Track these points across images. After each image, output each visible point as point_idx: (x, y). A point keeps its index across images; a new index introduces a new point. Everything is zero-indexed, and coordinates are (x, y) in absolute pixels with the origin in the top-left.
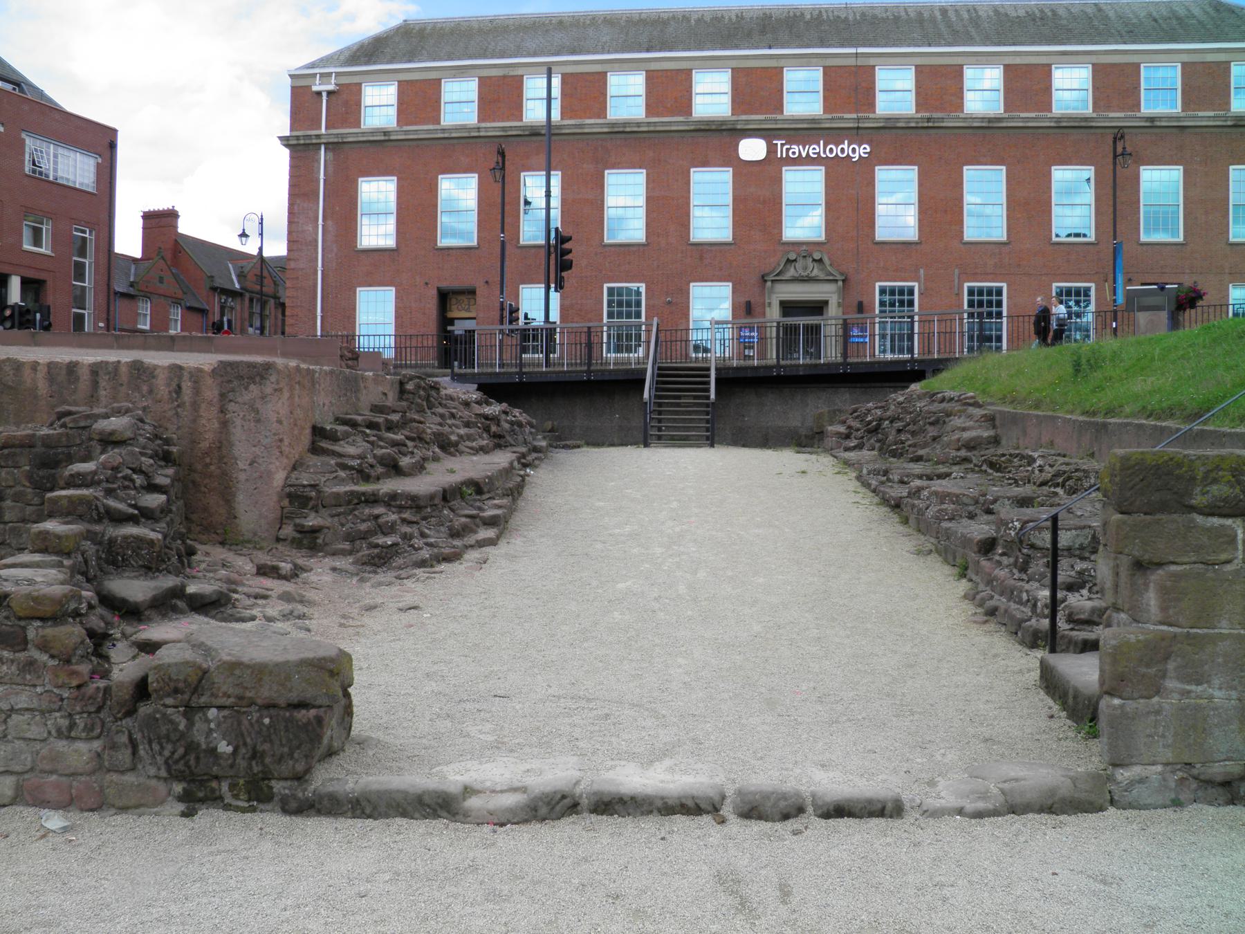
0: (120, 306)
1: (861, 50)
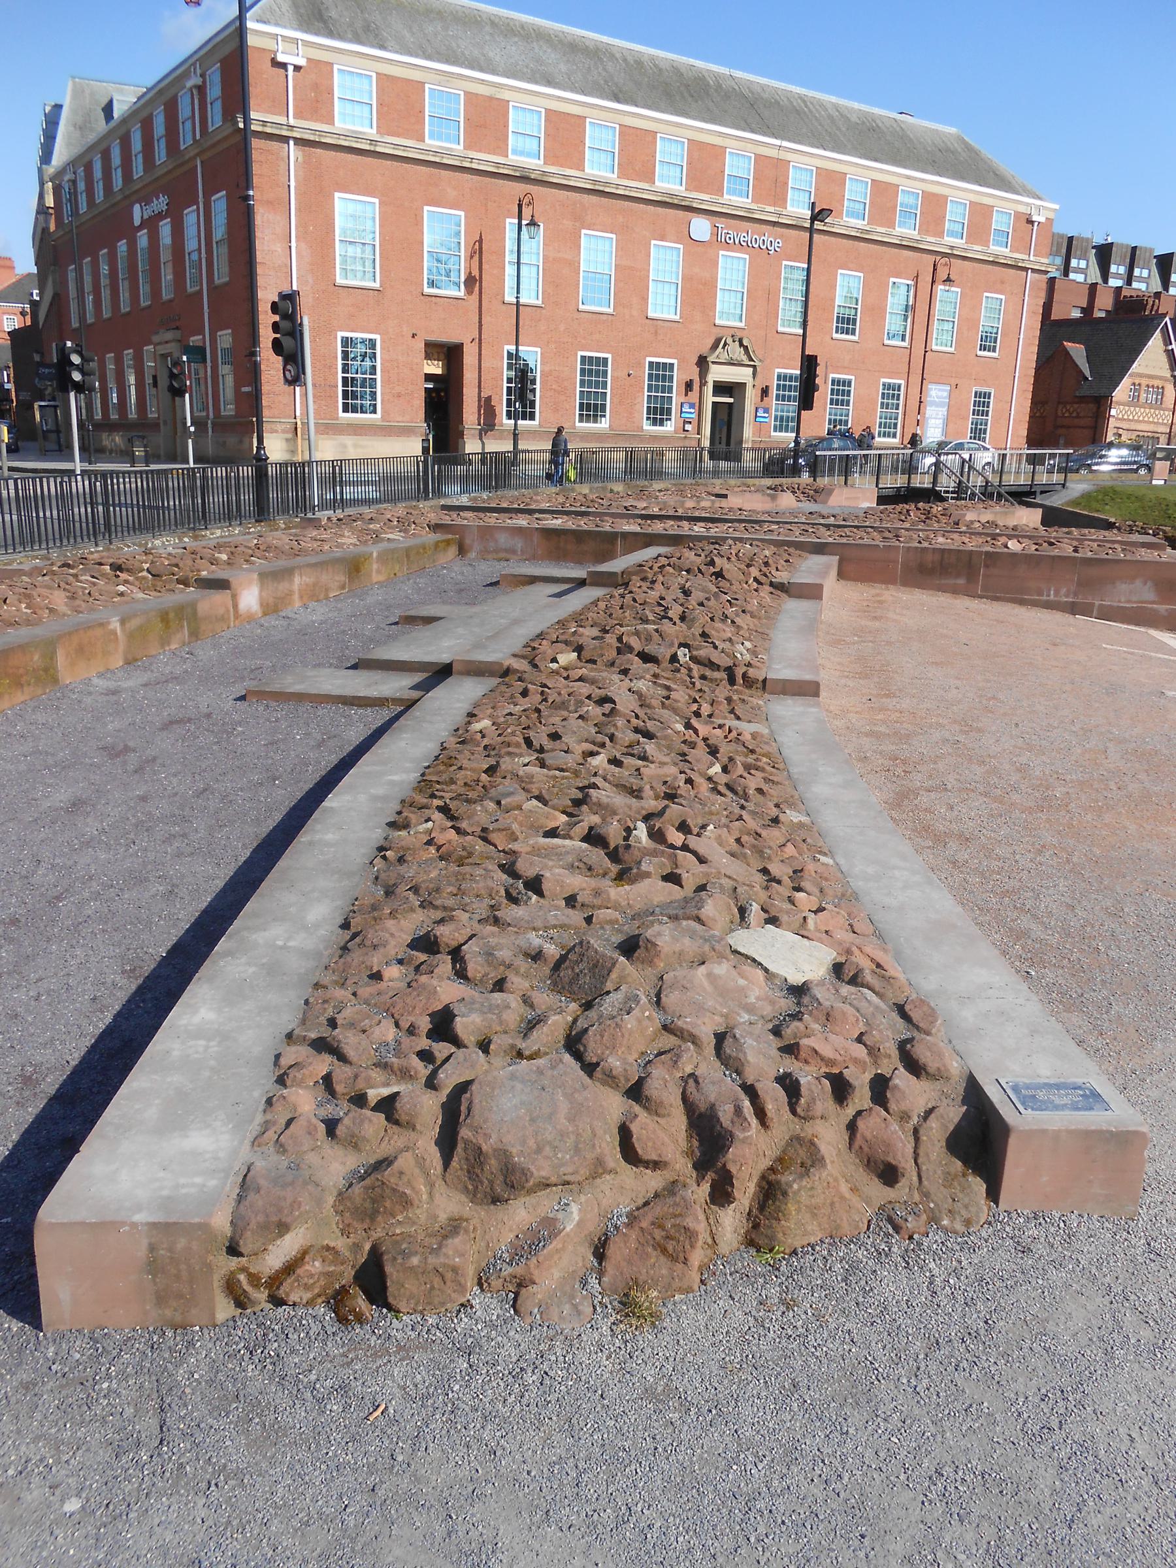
1: (785, 144)
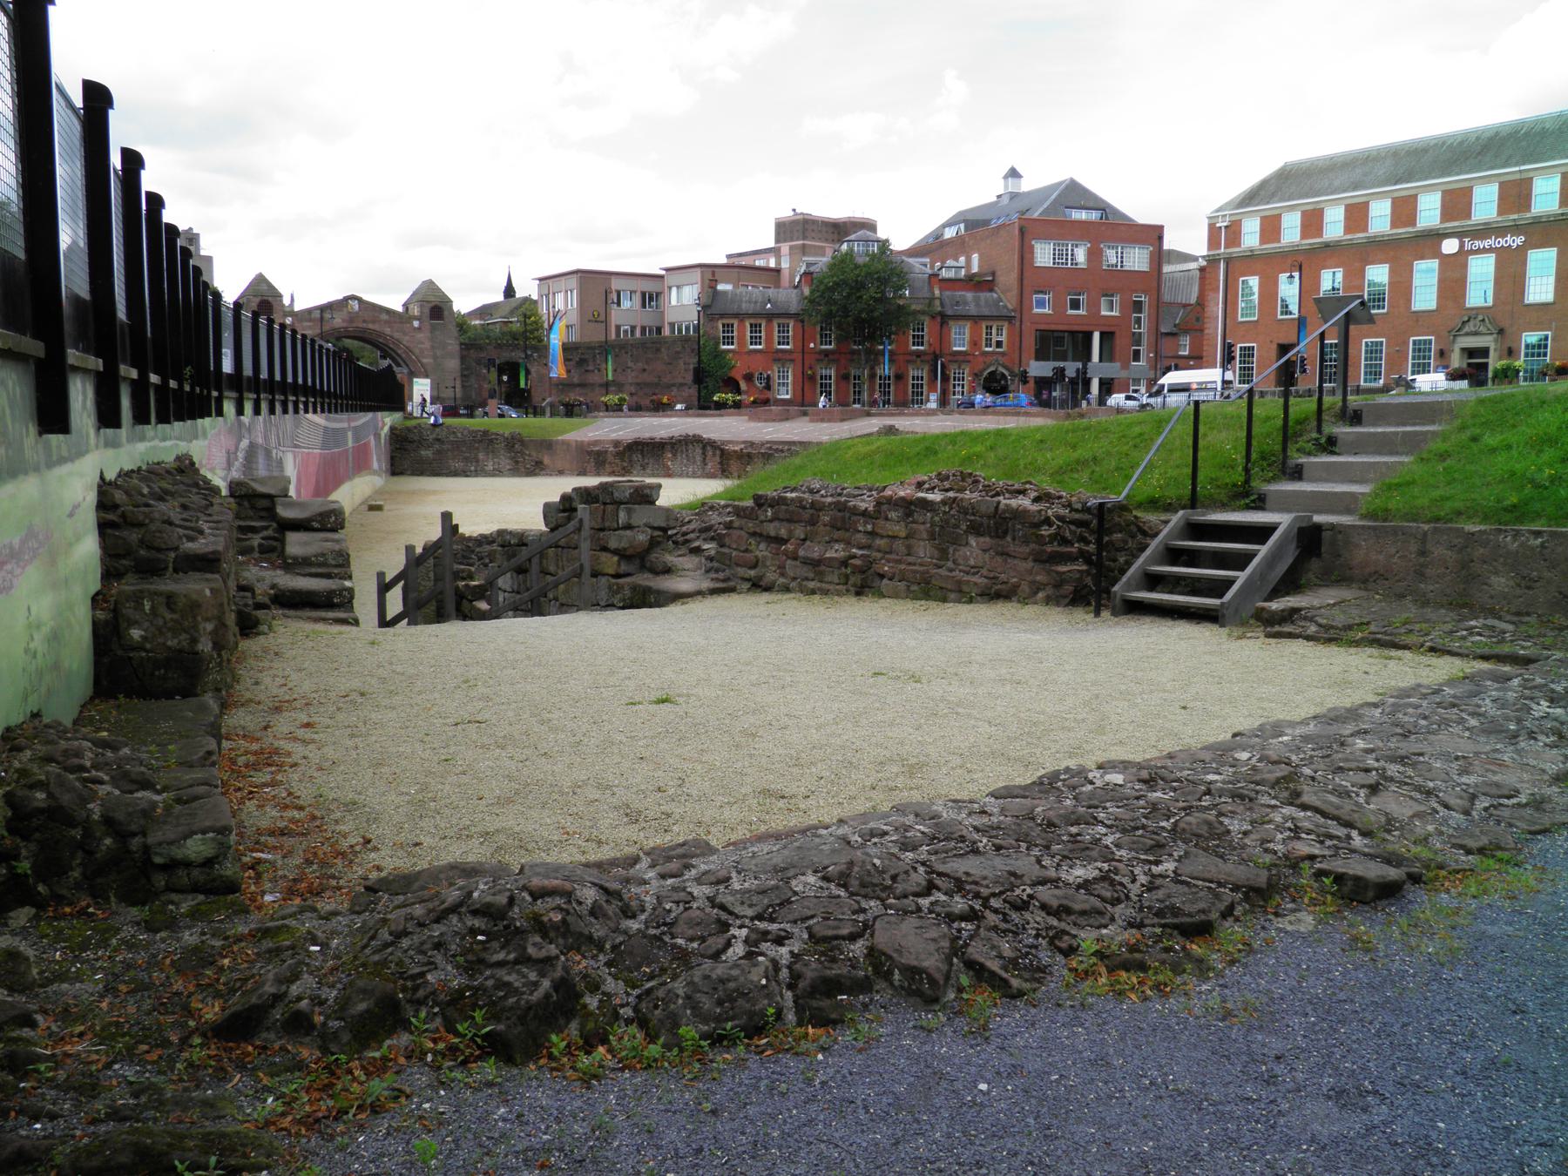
0: (1166, 344)
